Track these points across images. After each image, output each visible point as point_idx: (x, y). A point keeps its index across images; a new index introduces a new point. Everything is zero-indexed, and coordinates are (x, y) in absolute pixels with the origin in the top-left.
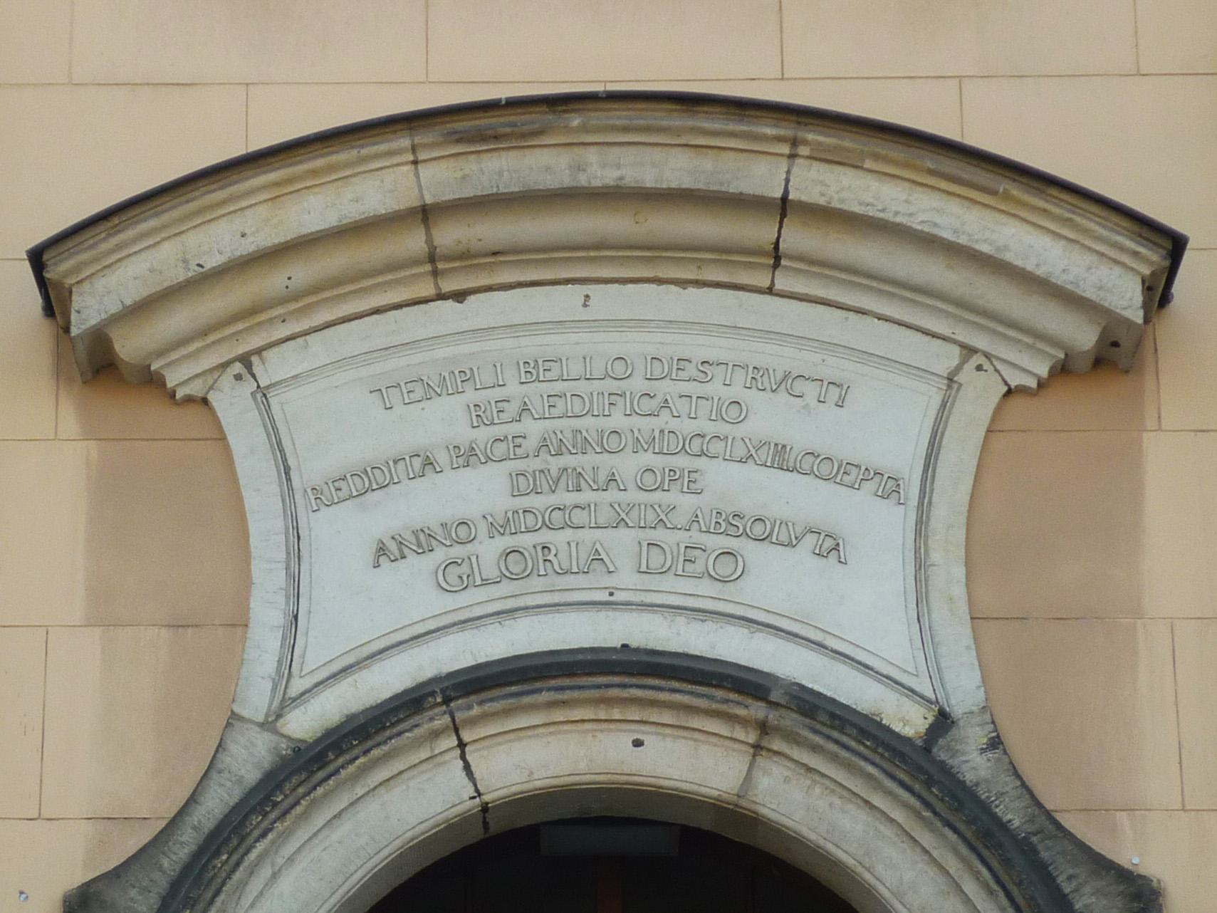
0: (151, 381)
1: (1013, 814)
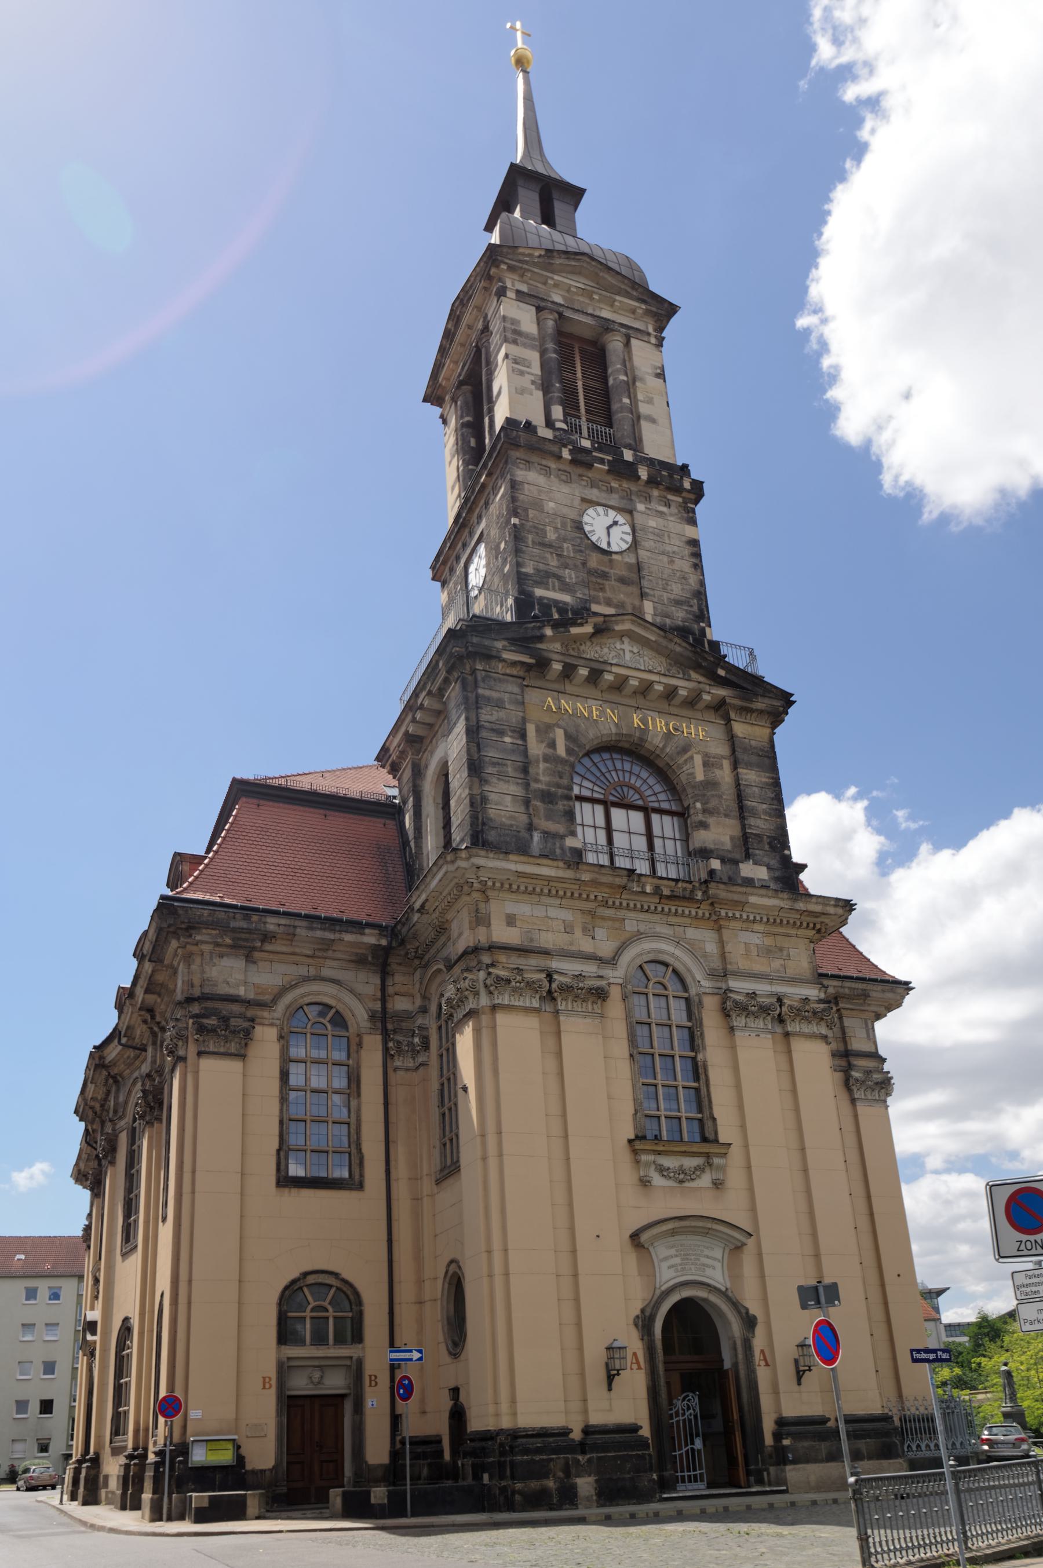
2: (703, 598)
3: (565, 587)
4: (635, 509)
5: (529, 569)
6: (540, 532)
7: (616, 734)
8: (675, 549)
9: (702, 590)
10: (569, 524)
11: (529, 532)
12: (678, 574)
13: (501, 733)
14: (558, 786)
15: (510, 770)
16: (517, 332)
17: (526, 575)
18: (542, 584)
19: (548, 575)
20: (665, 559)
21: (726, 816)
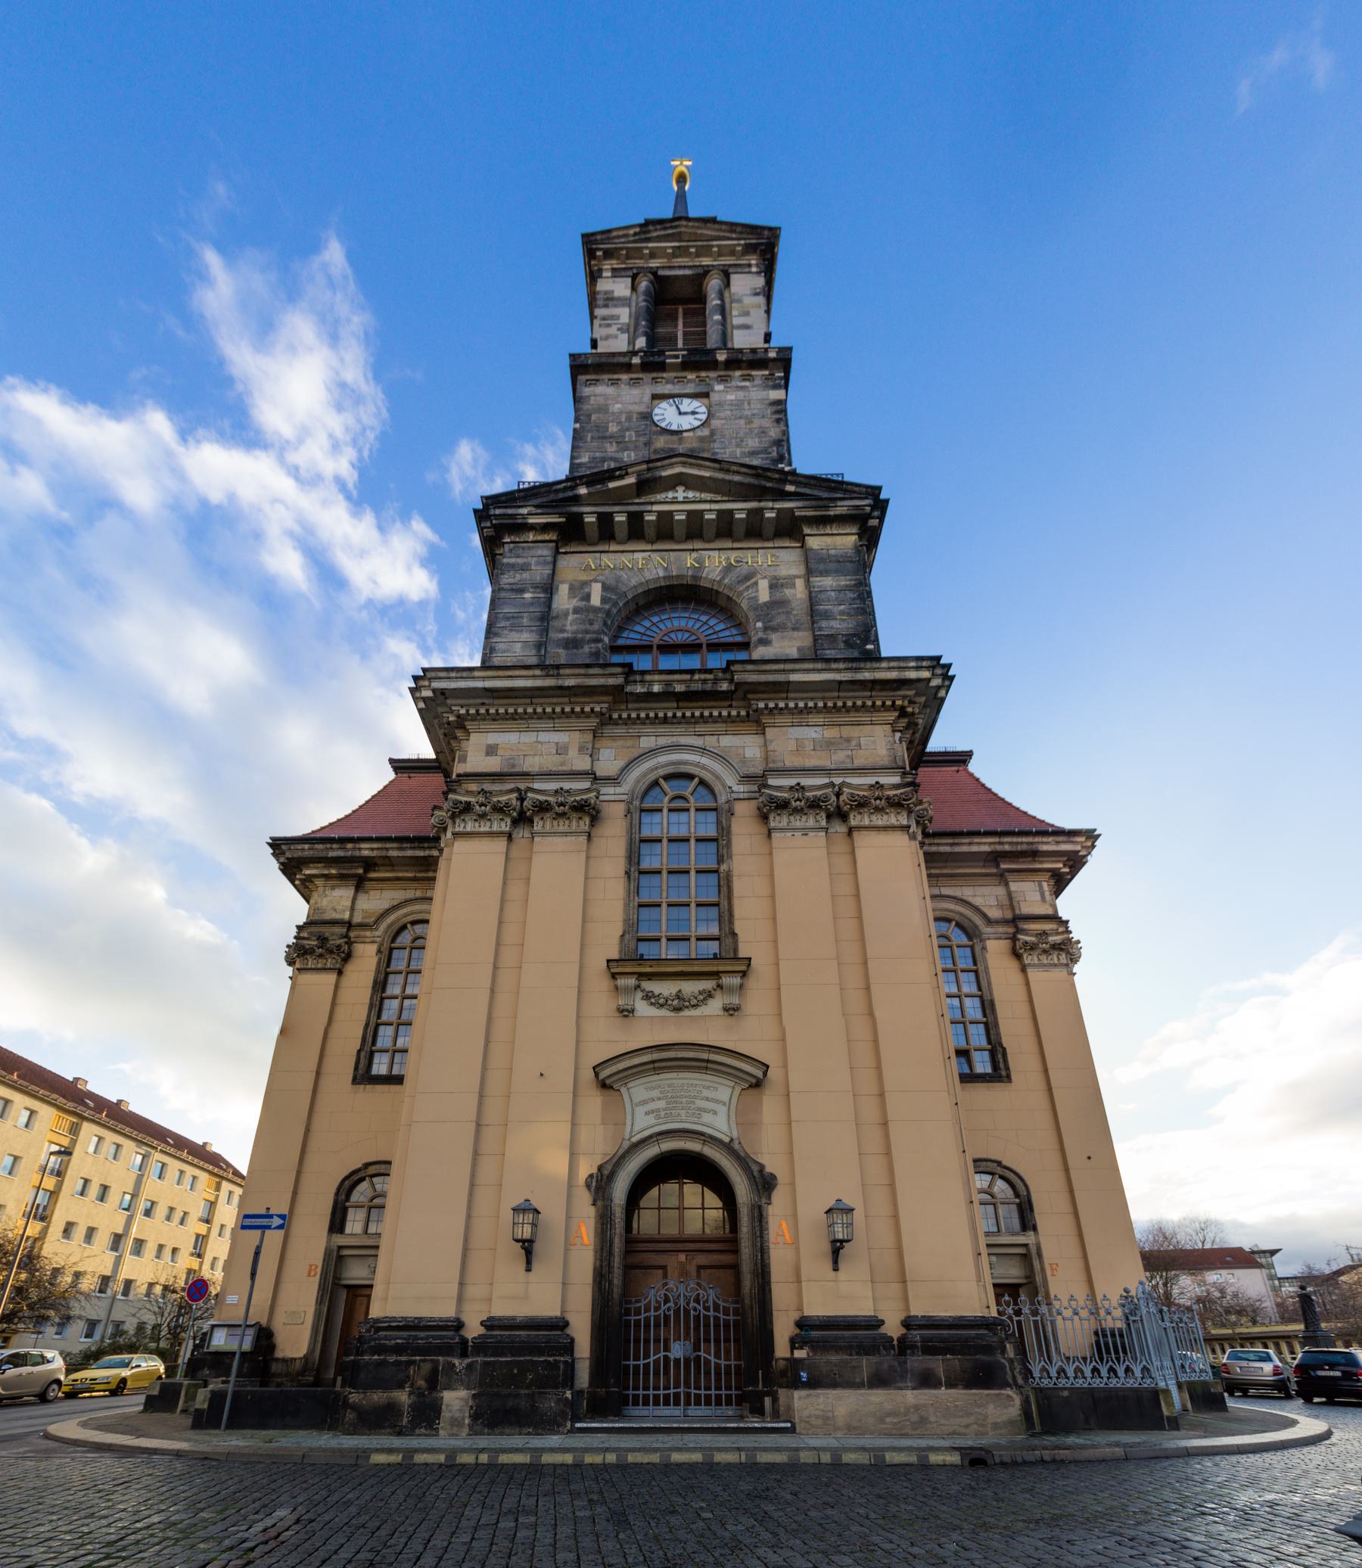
0: (611, 1087)
1: (742, 1154)
7: (664, 578)
13: (522, 591)
14: (587, 632)
15: (525, 621)
21: (794, 629)
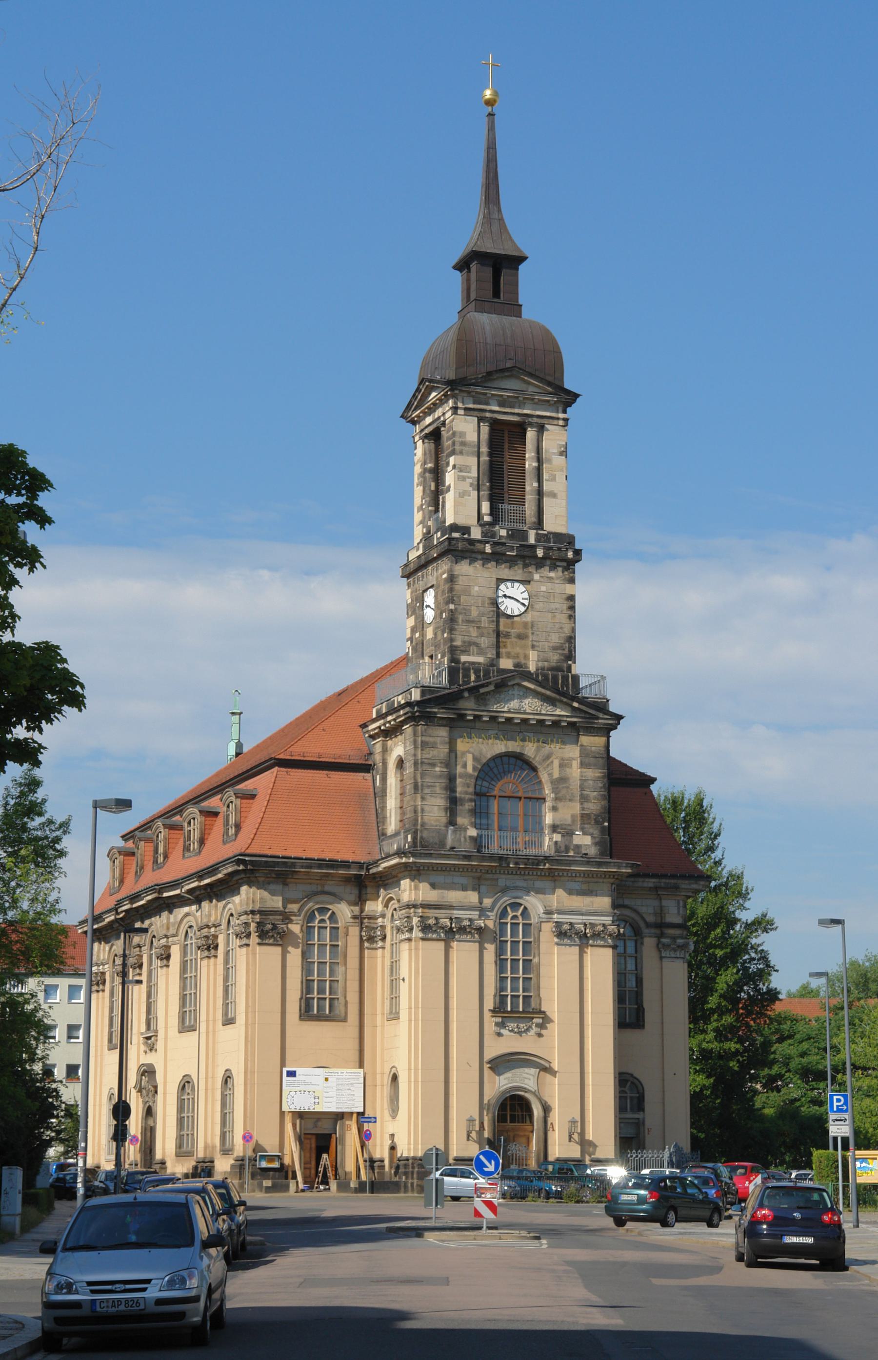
2: (573, 641)
3: (481, 652)
4: (533, 580)
5: (458, 643)
6: (467, 611)
8: (558, 606)
9: (573, 635)
10: (487, 601)
11: (460, 613)
12: (557, 626)
16: (463, 444)
17: (456, 647)
18: (465, 652)
19: (471, 644)
20: (550, 615)
